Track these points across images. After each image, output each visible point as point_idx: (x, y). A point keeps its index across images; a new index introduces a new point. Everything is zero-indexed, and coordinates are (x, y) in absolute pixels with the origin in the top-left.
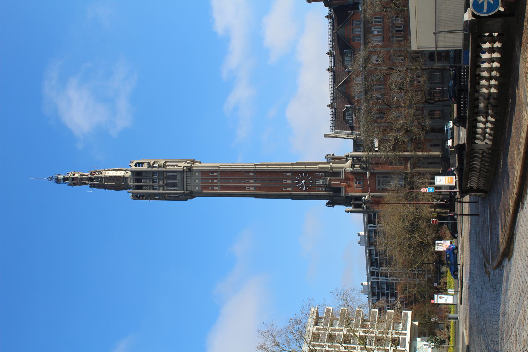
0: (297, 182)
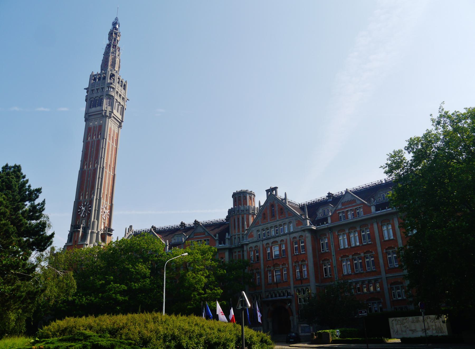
0: (85, 204)
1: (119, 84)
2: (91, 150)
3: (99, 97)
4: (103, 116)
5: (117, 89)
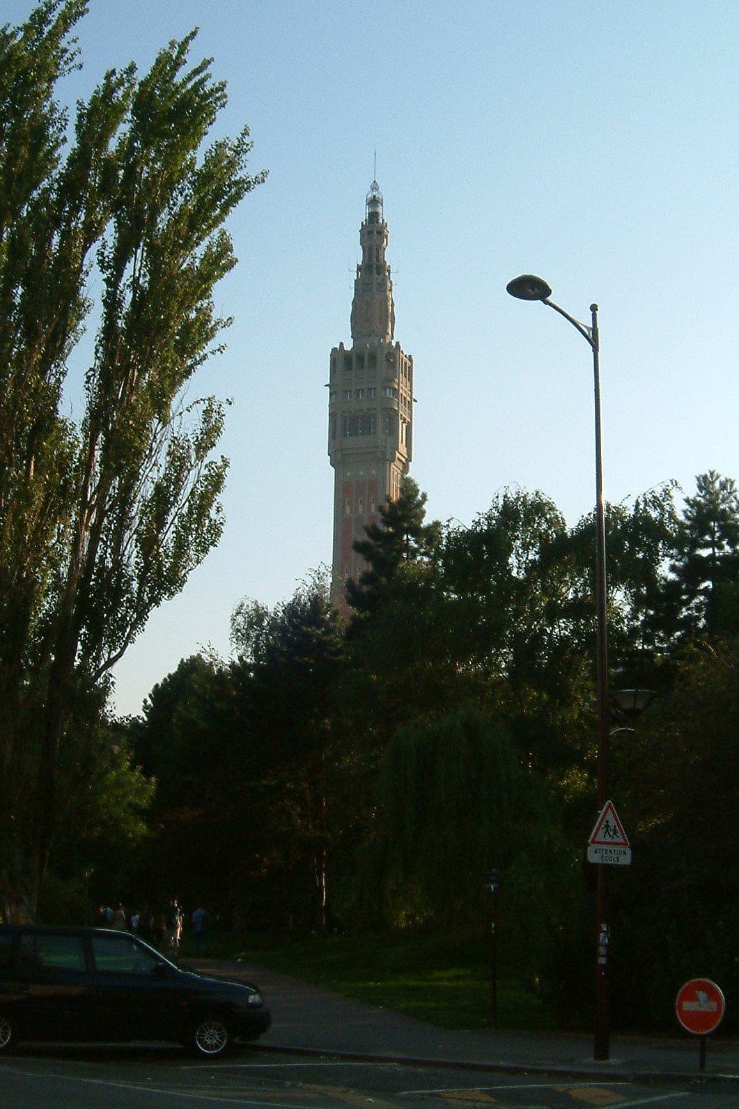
3: (365, 411)
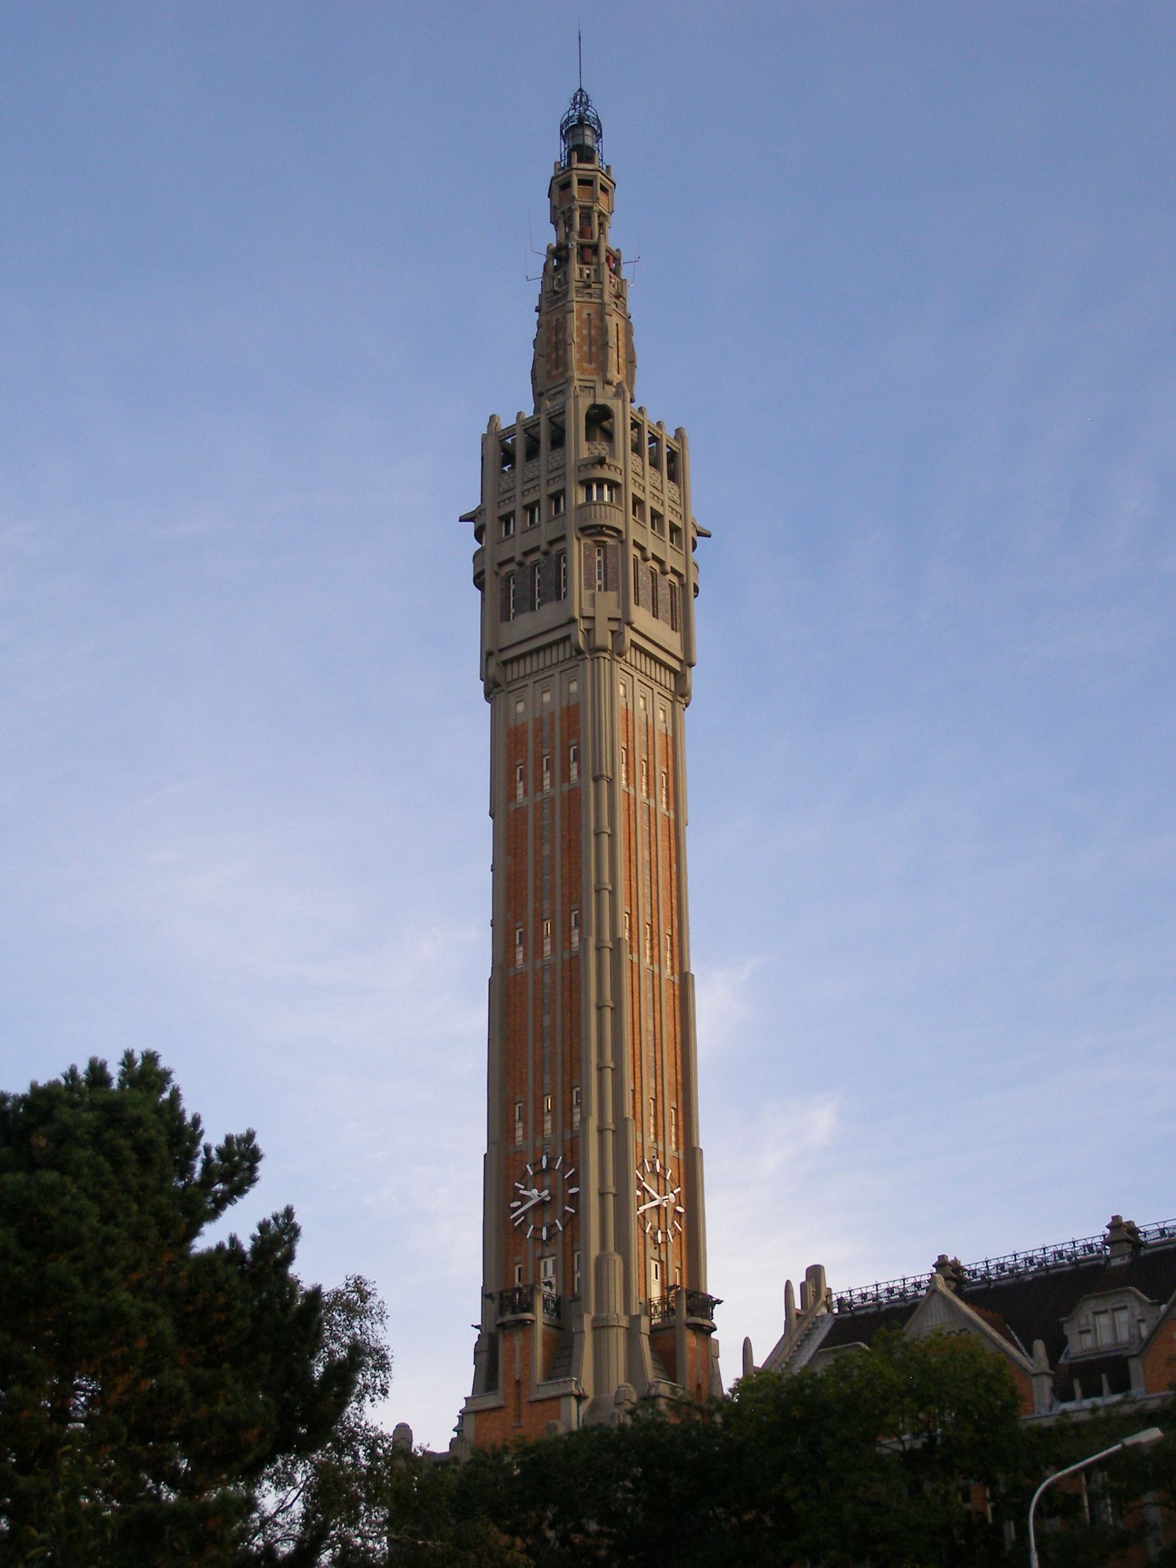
1: (641, 456)
2: (537, 852)
3: (544, 547)
4: (579, 652)
5: (632, 489)
